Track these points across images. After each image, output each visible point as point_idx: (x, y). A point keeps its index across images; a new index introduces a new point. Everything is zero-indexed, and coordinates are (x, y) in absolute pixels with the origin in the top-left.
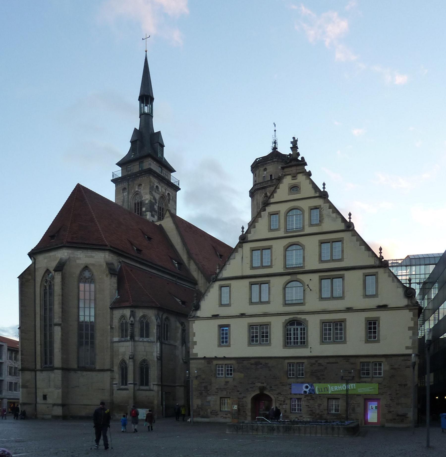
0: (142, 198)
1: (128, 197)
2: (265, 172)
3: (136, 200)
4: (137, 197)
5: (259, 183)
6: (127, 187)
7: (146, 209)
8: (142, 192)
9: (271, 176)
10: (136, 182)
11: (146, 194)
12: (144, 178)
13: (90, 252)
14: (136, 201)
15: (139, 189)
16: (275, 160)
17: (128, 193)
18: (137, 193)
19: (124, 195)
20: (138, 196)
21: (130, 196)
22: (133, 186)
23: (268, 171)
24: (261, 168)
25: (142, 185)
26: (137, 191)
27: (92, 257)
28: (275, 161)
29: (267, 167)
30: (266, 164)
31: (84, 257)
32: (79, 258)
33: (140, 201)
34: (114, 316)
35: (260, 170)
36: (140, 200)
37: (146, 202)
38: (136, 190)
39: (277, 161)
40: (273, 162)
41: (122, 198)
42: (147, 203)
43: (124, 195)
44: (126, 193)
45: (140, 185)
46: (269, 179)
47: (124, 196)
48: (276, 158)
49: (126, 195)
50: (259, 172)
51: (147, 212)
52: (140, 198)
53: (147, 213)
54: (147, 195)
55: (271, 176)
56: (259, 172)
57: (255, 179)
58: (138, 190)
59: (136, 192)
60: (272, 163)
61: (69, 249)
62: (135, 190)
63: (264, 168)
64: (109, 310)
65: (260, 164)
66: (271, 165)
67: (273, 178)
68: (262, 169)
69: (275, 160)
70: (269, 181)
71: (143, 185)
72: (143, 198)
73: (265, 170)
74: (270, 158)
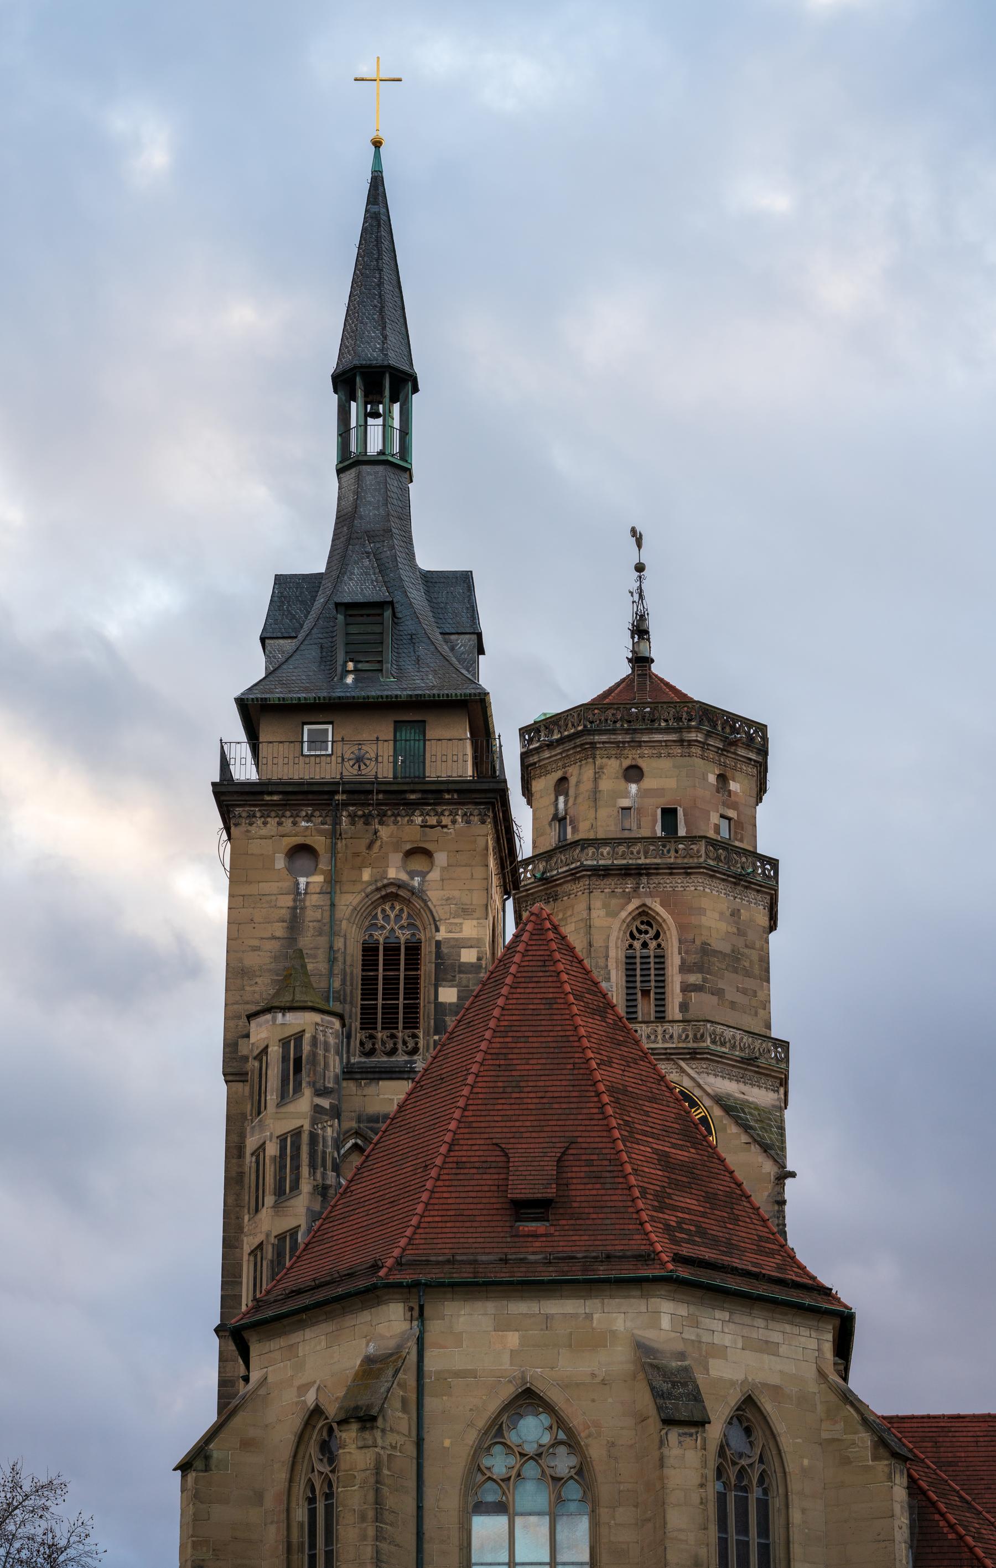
0: (437, 930)
1: (333, 905)
2: (633, 788)
4: (383, 911)
5: (596, 843)
6: (319, 842)
7: (459, 997)
8: (434, 895)
9: (669, 814)
12: (446, 820)
14: (380, 936)
15: (412, 874)
16: (692, 736)
17: (333, 884)
18: (393, 890)
19: (297, 884)
20: (392, 908)
22: (370, 847)
23: (648, 783)
24: (605, 760)
25: (428, 854)
26: (400, 885)
29: (642, 763)
30: (640, 744)
31: (740, 1345)
32: (720, 1352)
33: (403, 940)
35: (601, 768)
36: (403, 936)
37: (463, 959)
38: (392, 873)
39: (704, 745)
40: (681, 742)
41: (287, 901)
42: (472, 965)
43: (302, 886)
44: (318, 879)
46: (659, 832)
47: (299, 894)
48: (698, 729)
49: (314, 888)
50: (596, 780)
54: (475, 922)
55: (669, 814)
56: (596, 780)
57: (561, 805)
58: (404, 877)
59: (391, 884)
61: (798, 1320)
62: (385, 872)
63: (627, 763)
65: (604, 738)
66: (669, 755)
67: (682, 832)
68: (613, 766)
69: (692, 736)
70: (653, 839)
71: (441, 858)
72: (442, 928)
73: (634, 773)
74: (666, 721)
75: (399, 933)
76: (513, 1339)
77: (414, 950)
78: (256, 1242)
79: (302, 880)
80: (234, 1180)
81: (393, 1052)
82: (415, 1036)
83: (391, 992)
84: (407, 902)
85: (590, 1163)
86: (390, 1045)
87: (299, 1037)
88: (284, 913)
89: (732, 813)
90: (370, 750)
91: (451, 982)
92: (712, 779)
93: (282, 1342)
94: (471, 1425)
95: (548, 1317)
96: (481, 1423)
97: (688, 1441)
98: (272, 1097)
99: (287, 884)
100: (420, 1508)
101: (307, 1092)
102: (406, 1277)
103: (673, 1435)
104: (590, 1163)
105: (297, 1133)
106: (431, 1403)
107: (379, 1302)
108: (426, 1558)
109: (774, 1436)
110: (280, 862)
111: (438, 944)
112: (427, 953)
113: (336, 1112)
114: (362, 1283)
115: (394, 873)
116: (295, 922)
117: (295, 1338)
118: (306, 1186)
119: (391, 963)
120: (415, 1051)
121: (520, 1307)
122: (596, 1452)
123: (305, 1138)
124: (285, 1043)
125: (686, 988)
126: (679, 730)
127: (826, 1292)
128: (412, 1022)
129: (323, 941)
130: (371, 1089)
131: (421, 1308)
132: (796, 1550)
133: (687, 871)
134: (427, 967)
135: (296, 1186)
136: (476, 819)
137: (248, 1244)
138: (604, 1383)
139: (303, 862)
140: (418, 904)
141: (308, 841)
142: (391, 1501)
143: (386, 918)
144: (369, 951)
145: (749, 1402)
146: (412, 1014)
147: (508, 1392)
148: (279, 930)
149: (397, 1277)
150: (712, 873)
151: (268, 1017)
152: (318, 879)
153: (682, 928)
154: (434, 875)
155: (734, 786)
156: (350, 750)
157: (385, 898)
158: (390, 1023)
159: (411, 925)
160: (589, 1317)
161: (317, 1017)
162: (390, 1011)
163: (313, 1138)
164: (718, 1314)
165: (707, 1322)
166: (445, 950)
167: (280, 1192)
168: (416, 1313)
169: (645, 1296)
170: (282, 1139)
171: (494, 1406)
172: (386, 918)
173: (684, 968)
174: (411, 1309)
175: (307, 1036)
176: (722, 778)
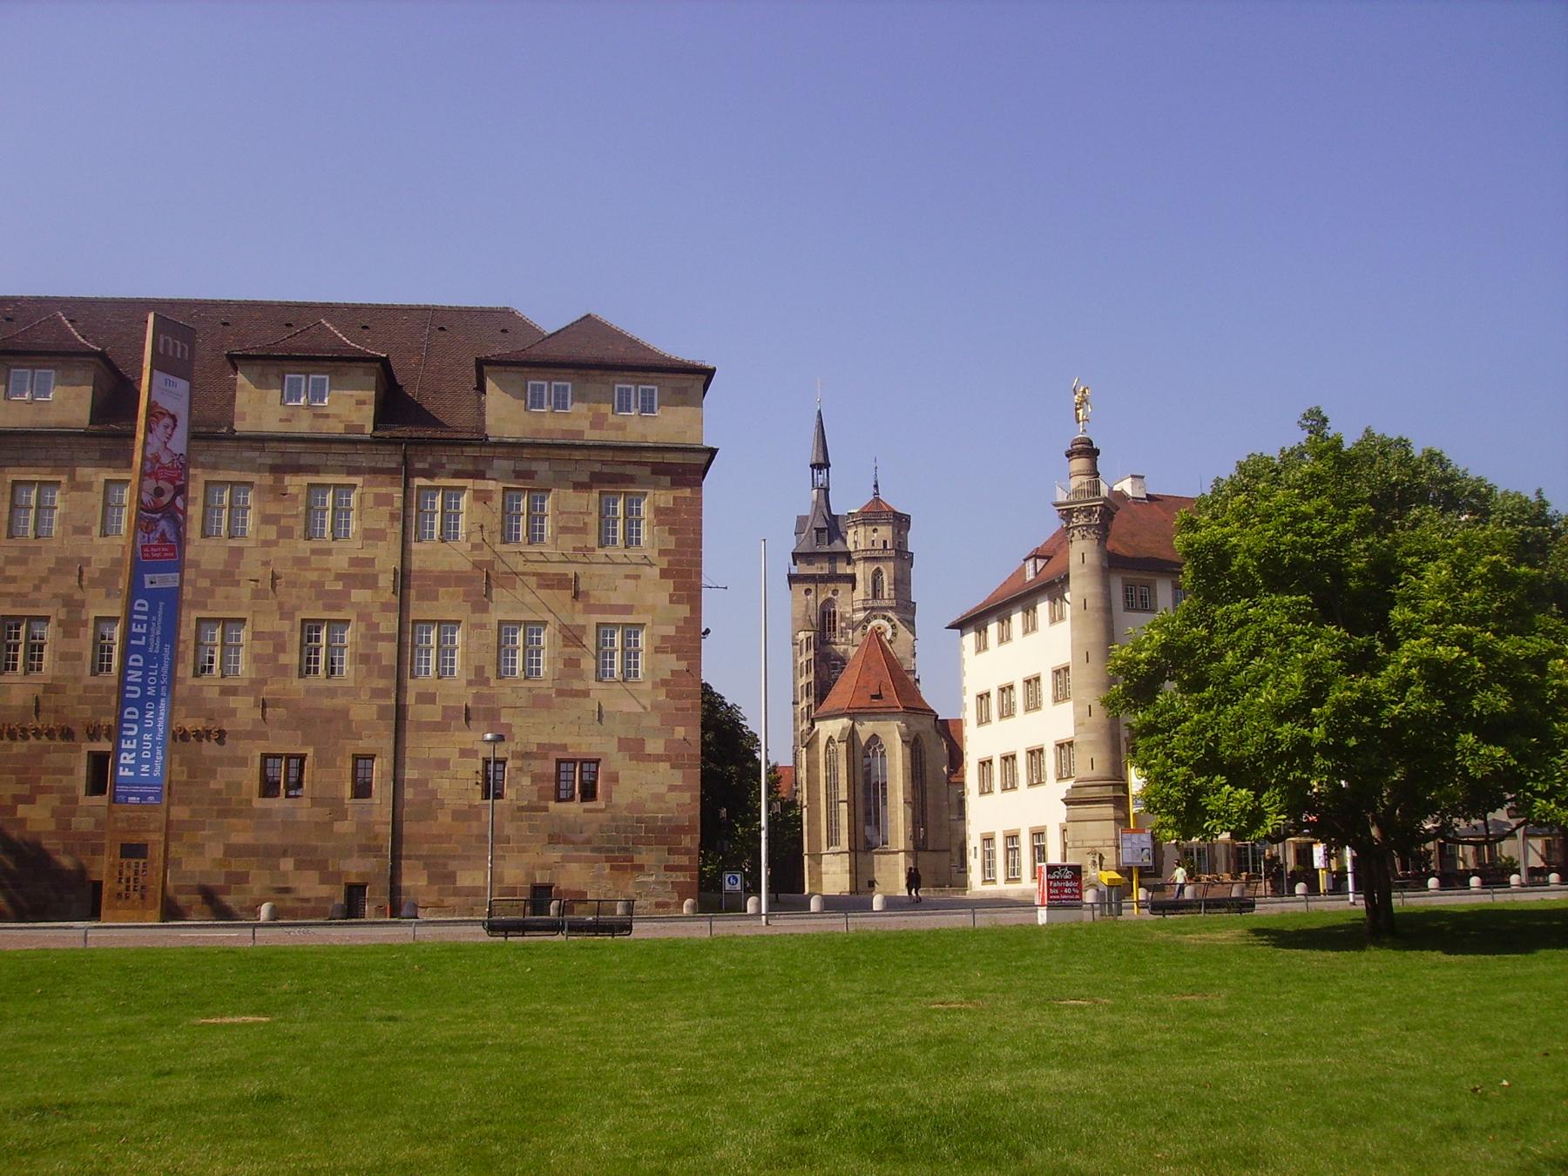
9: (885, 542)
36: (832, 610)
55: (885, 542)
68: (871, 528)
73: (875, 530)
77: (835, 613)
80: (795, 668)
83: (829, 624)
102: (851, 711)
115: (830, 595)
116: (807, 606)
119: (829, 617)
125: (889, 589)
127: (932, 711)
128: (834, 630)
145: (918, 734)
153: (888, 573)
162: (829, 628)
173: (889, 584)
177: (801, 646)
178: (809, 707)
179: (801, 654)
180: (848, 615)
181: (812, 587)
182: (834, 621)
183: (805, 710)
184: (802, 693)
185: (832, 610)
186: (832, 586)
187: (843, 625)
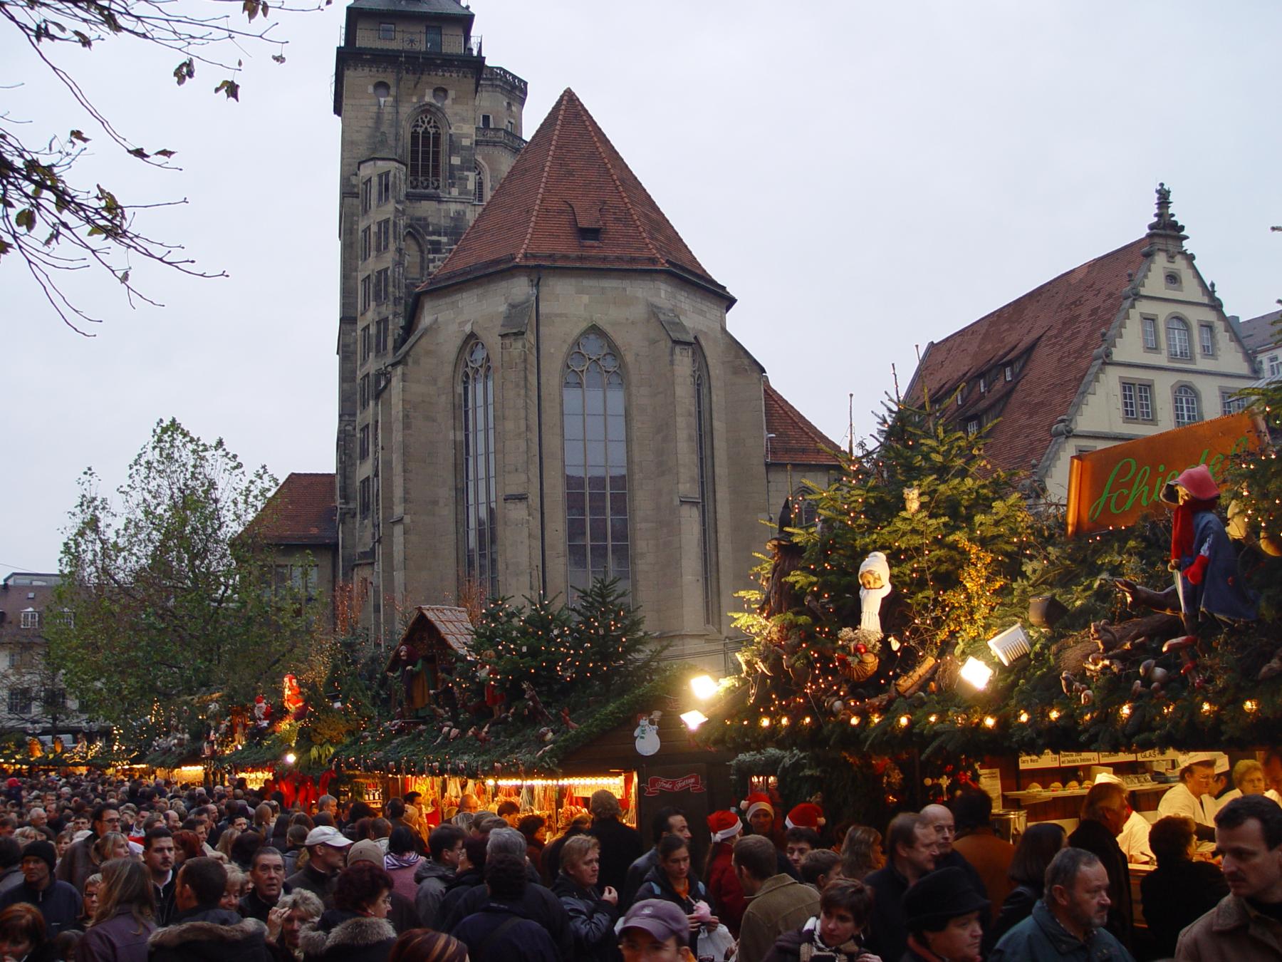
1: (397, 112)
3: (417, 126)
10: (425, 78)
11: (464, 120)
13: (699, 300)
16: (498, 83)
17: (397, 100)
21: (406, 110)
25: (445, 91)
26: (431, 105)
27: (702, 313)
28: (497, 86)
34: (772, 486)
40: (492, 85)
41: (375, 109)
44: (390, 99)
45: (441, 92)
51: (469, 169)
52: (432, 124)
53: (466, 173)
58: (433, 101)
60: (490, 89)
64: (763, 469)
67: (492, 126)
71: (452, 94)
75: (429, 129)
76: (585, 298)
77: (437, 137)
78: (367, 274)
79: (382, 100)
81: (427, 187)
82: (438, 180)
84: (434, 114)
85: (615, 213)
86: (425, 184)
87: (387, 174)
88: (374, 116)
89: (512, 121)
90: (417, 37)
91: (458, 154)
92: (505, 104)
93: (448, 300)
94: (564, 341)
95: (603, 288)
96: (570, 341)
97: (685, 353)
98: (374, 202)
99: (374, 101)
100: (539, 383)
101: (392, 201)
102: (532, 263)
103: (678, 349)
104: (615, 213)
105: (387, 221)
106: (542, 329)
107: (513, 276)
108: (543, 410)
109: (705, 357)
110: (371, 89)
111: (451, 135)
112: (444, 140)
113: (403, 212)
114: (503, 266)
115: (428, 98)
116: (378, 118)
117: (458, 297)
118: (392, 247)
120: (438, 188)
121: (588, 283)
122: (629, 358)
123: (391, 223)
124: (380, 176)
126: (491, 80)
128: (436, 174)
129: (393, 130)
130: (417, 205)
131: (539, 279)
132: (715, 415)
133: (495, 144)
134: (444, 146)
135: (386, 247)
136: (469, 76)
137: (361, 276)
138: (633, 323)
139: (382, 91)
140: (440, 115)
141: (385, 81)
142: (530, 378)
143: (423, 122)
144: (414, 136)
146: (436, 167)
147: (584, 326)
148: (371, 123)
149: (523, 263)
150: (506, 146)
151: (372, 163)
152: (390, 99)
153: (492, 170)
154: (448, 102)
155: (514, 108)
156: (407, 36)
157: (423, 112)
158: (425, 173)
159: (435, 127)
160: (625, 289)
161: (396, 165)
163: (395, 224)
164: (683, 293)
165: (678, 296)
166: (454, 139)
167: (378, 249)
168: (535, 282)
169: (653, 280)
170: (379, 224)
171: (576, 332)
172: (423, 122)
174: (532, 281)
175: (391, 174)
176: (509, 104)
177: (367, 192)
178: (382, 322)
179: (366, 211)
180: (466, 142)
181: (389, 78)
182: (436, 154)
183: (373, 330)
184: (366, 295)
185: (432, 131)
186: (437, 79)
187: (456, 160)
